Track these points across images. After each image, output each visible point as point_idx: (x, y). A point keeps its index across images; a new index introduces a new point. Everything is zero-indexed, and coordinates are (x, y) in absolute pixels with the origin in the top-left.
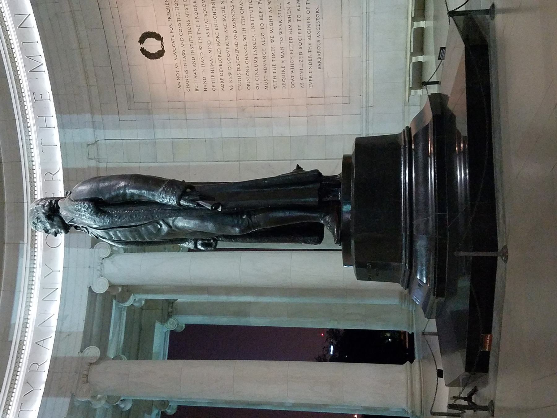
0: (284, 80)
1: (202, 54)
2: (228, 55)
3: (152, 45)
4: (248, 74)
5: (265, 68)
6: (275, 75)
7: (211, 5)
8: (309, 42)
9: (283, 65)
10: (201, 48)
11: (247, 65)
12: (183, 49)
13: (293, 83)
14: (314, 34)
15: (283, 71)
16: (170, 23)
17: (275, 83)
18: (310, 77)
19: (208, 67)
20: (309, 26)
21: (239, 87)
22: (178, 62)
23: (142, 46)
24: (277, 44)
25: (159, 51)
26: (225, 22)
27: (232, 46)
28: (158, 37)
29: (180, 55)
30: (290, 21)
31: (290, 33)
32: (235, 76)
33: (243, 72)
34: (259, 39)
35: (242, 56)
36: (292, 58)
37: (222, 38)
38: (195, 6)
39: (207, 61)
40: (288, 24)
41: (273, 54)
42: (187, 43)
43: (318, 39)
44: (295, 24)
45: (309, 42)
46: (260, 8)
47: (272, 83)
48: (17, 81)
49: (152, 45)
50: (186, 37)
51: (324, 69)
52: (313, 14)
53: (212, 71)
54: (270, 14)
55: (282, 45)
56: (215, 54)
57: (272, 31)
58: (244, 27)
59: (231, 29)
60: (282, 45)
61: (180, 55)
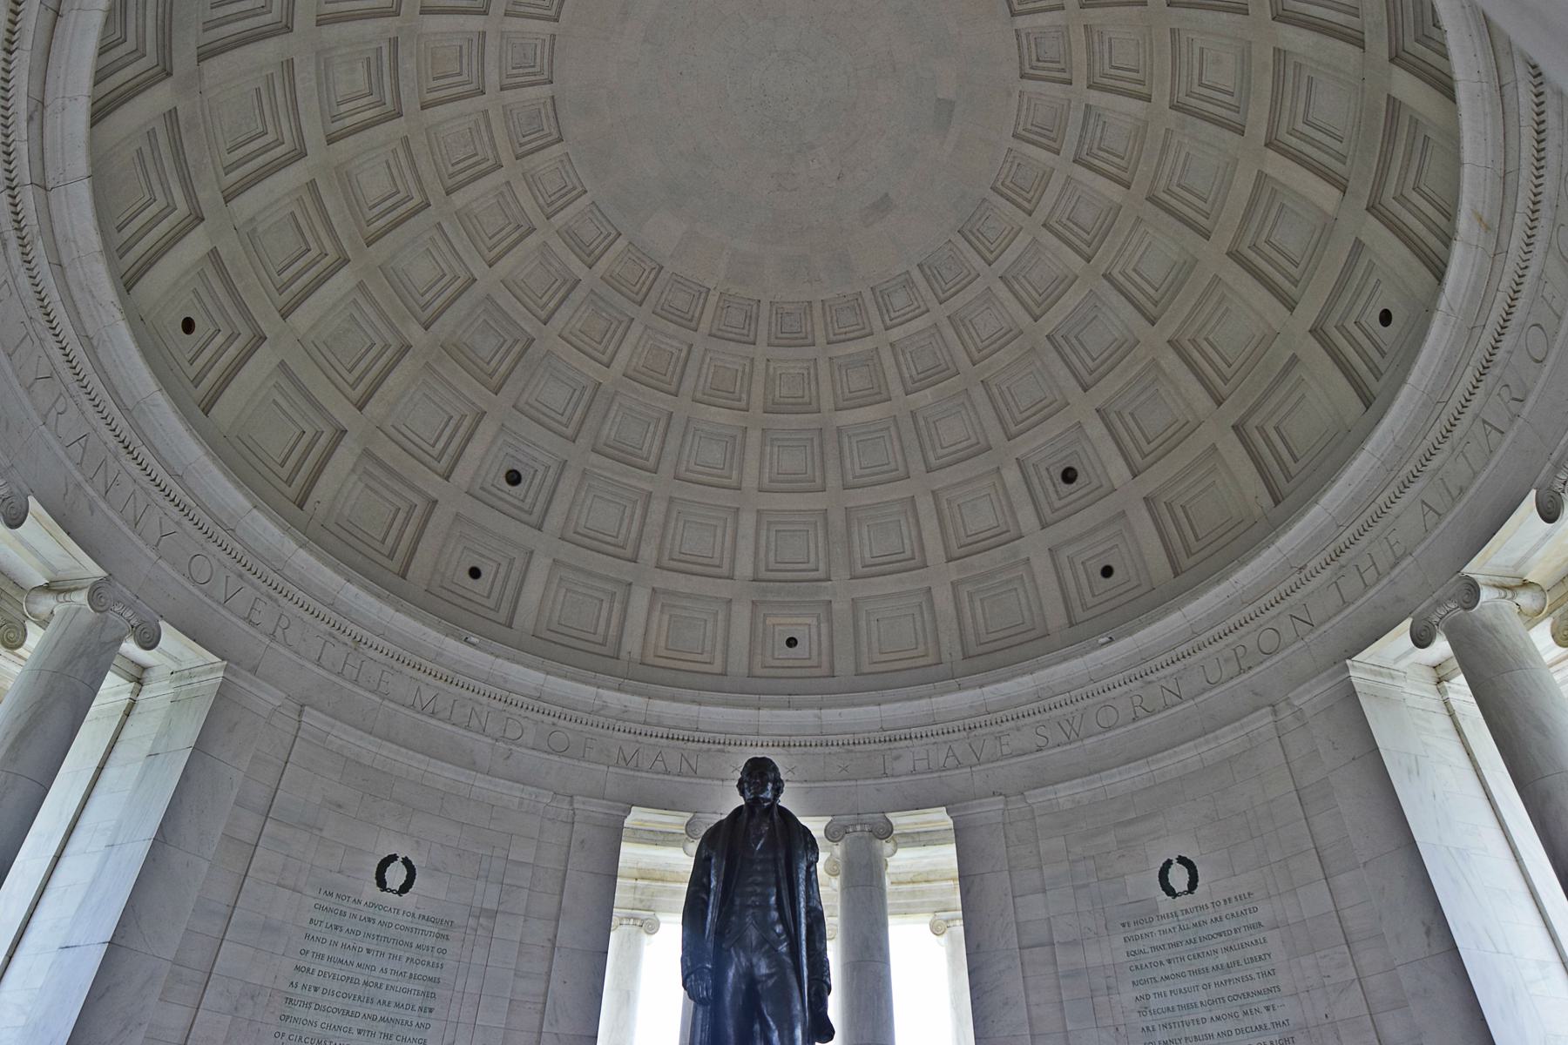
2: (347, 996)
3: (396, 875)
7: (422, 989)
10: (368, 951)
19: (339, 953)
22: (361, 907)
27: (355, 1006)
28: (405, 888)
29: (370, 913)
33: (312, 1015)
35: (335, 1019)
39: (348, 956)
49: (396, 875)
50: (392, 933)
56: (354, 972)
59: (380, 1011)
61: (370, 913)
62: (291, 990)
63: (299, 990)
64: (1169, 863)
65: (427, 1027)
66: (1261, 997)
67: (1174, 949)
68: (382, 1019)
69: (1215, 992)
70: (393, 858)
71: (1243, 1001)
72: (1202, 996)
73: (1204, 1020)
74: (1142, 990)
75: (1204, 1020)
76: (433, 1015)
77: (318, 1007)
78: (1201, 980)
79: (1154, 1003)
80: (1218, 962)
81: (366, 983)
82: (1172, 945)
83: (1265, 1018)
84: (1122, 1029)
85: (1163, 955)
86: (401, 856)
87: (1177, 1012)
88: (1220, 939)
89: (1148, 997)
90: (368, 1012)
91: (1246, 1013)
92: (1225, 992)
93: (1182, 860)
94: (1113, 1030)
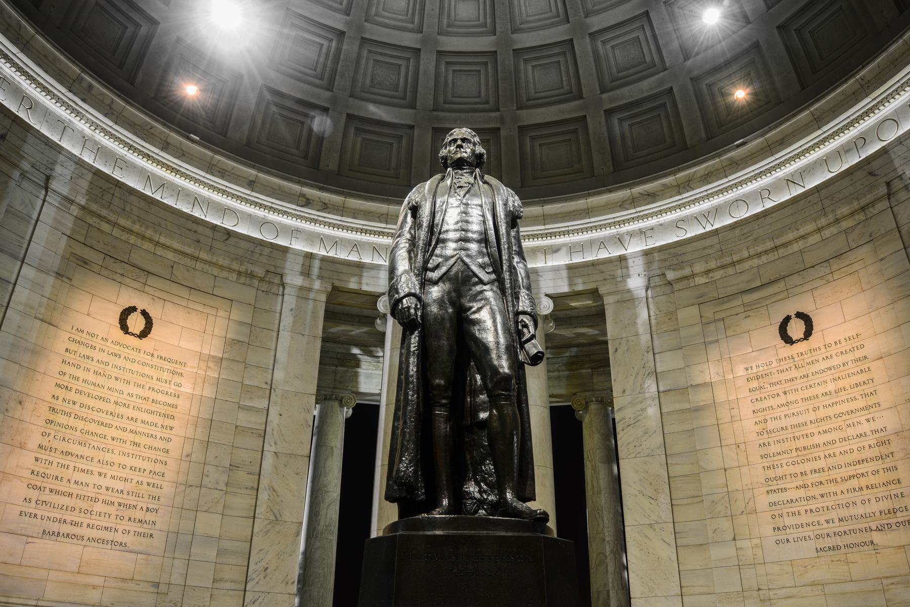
0: (44, 476)
1: (110, 377)
2: (100, 410)
3: (136, 323)
4: (67, 427)
5: (68, 453)
6: (55, 464)
8: (85, 525)
9: (65, 481)
10: (117, 379)
11: (79, 429)
12: (122, 357)
13: (35, 487)
14: (94, 533)
15: (57, 478)
16: (155, 356)
17: (44, 461)
18: (35, 516)
20: (106, 528)
21: (54, 409)
22: (109, 344)
23: (139, 311)
24: (94, 479)
25: (128, 328)
26: (139, 421)
27: (107, 419)
28: (144, 334)
30: (120, 505)
31: (104, 502)
32: (69, 408)
33: (72, 422)
34: (108, 457)
36: (70, 495)
37: (121, 410)
38: (167, 393)
39: (100, 380)
40: (116, 501)
41: (83, 471)
42: (128, 365)
43: (86, 538)
44: (111, 510)
45: (85, 525)
46: (144, 470)
47: (45, 457)
48: (148, 157)
49: (136, 323)
51: (41, 538)
52: (119, 537)
53: (85, 381)
54: (135, 481)
55: (91, 486)
57: (113, 477)
58: (128, 443)
59: (130, 426)
60: (91, 486)
62: (53, 401)
63: (60, 402)
64: (788, 319)
65: (169, 440)
66: (863, 413)
67: (789, 384)
68: (131, 431)
69: (822, 413)
70: (132, 309)
71: (847, 417)
72: (812, 416)
73: (812, 434)
74: (760, 416)
75: (812, 434)
76: (173, 432)
77: (77, 417)
78: (810, 405)
79: (771, 425)
80: (827, 390)
81: (116, 403)
82: (787, 381)
83: (866, 428)
84: (742, 446)
85: (778, 389)
86: (140, 307)
87: (790, 430)
88: (829, 372)
89: (766, 421)
90: (118, 424)
91: (849, 426)
92: (831, 411)
93: (799, 315)
94: (734, 447)
